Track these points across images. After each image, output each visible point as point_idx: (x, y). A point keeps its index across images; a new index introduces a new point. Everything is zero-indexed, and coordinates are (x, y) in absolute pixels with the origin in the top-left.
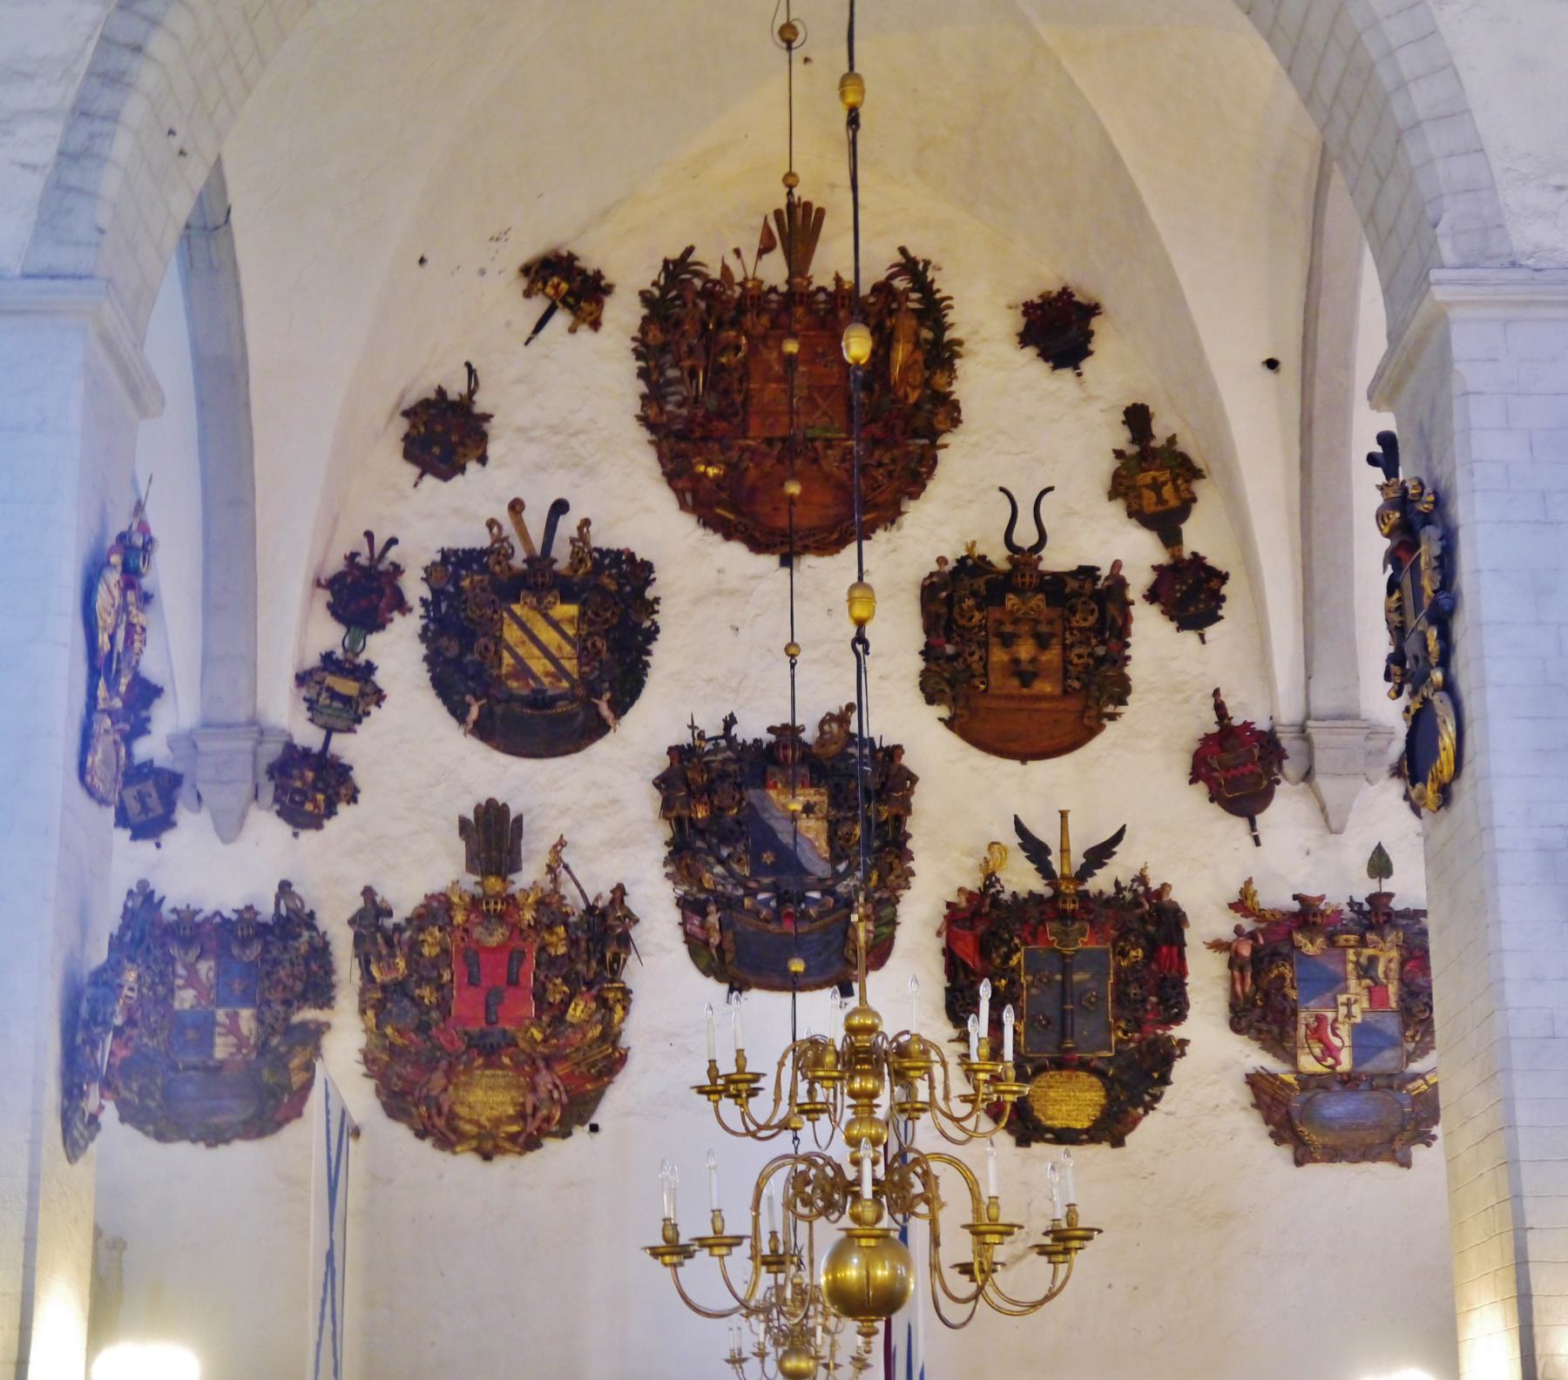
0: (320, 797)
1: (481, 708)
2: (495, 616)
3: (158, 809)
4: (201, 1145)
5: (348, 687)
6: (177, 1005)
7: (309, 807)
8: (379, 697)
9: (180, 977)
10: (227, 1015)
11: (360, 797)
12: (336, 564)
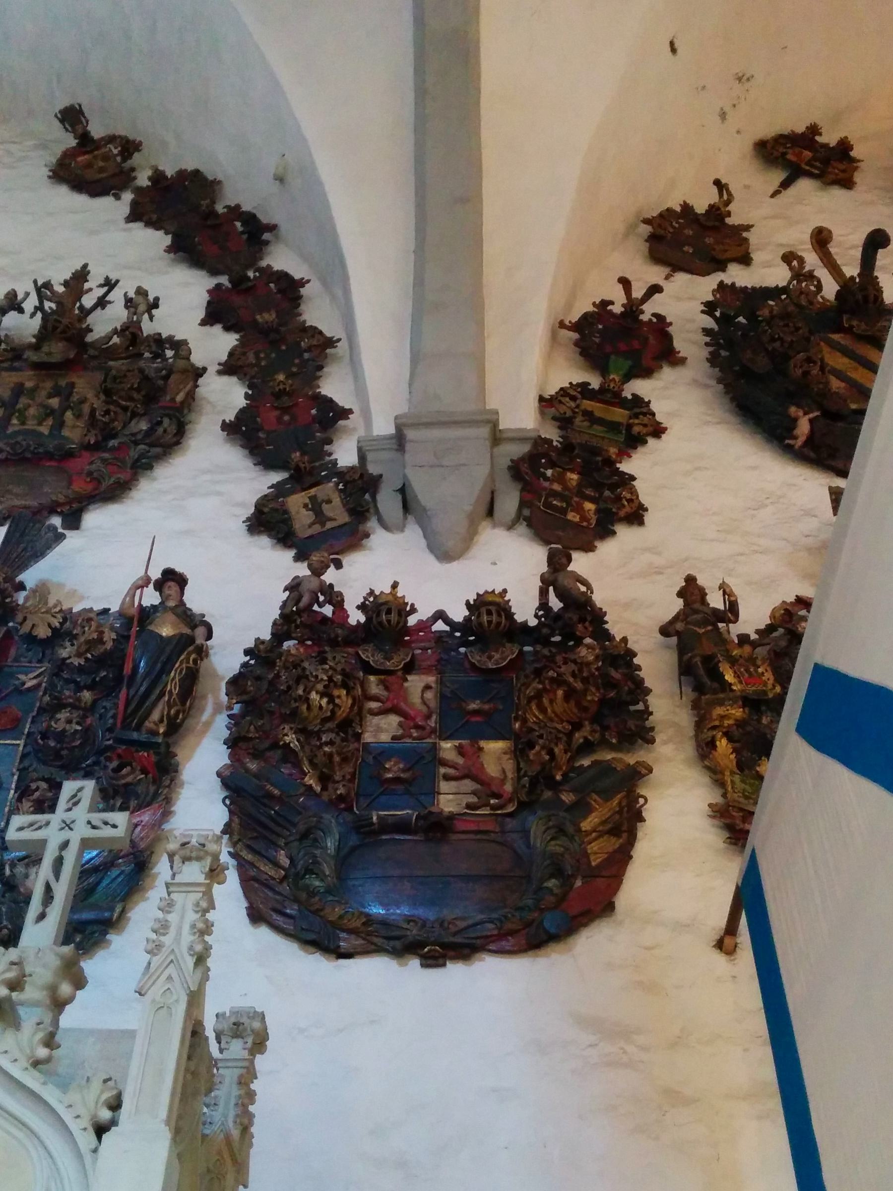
0: (589, 506)
1: (811, 421)
2: (812, 338)
3: (337, 513)
4: (415, 963)
5: (619, 415)
6: (368, 738)
7: (573, 517)
8: (658, 431)
9: (376, 699)
10: (460, 750)
11: (648, 518)
12: (584, 306)
